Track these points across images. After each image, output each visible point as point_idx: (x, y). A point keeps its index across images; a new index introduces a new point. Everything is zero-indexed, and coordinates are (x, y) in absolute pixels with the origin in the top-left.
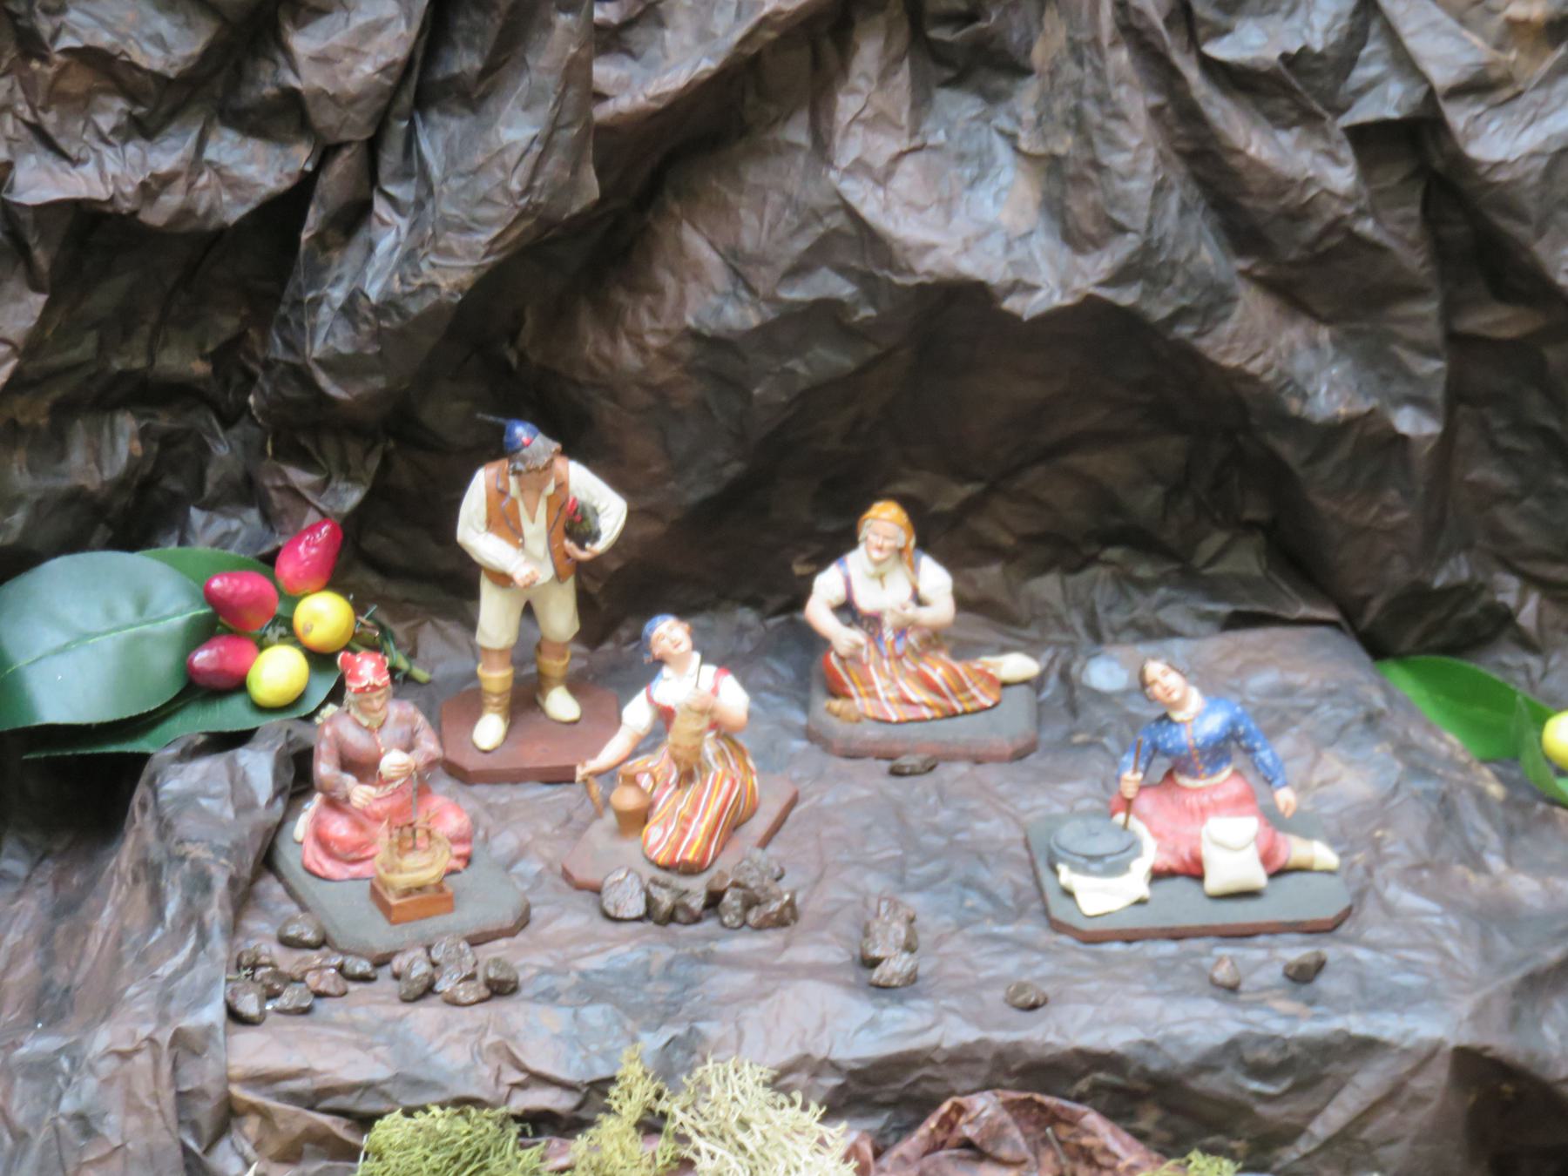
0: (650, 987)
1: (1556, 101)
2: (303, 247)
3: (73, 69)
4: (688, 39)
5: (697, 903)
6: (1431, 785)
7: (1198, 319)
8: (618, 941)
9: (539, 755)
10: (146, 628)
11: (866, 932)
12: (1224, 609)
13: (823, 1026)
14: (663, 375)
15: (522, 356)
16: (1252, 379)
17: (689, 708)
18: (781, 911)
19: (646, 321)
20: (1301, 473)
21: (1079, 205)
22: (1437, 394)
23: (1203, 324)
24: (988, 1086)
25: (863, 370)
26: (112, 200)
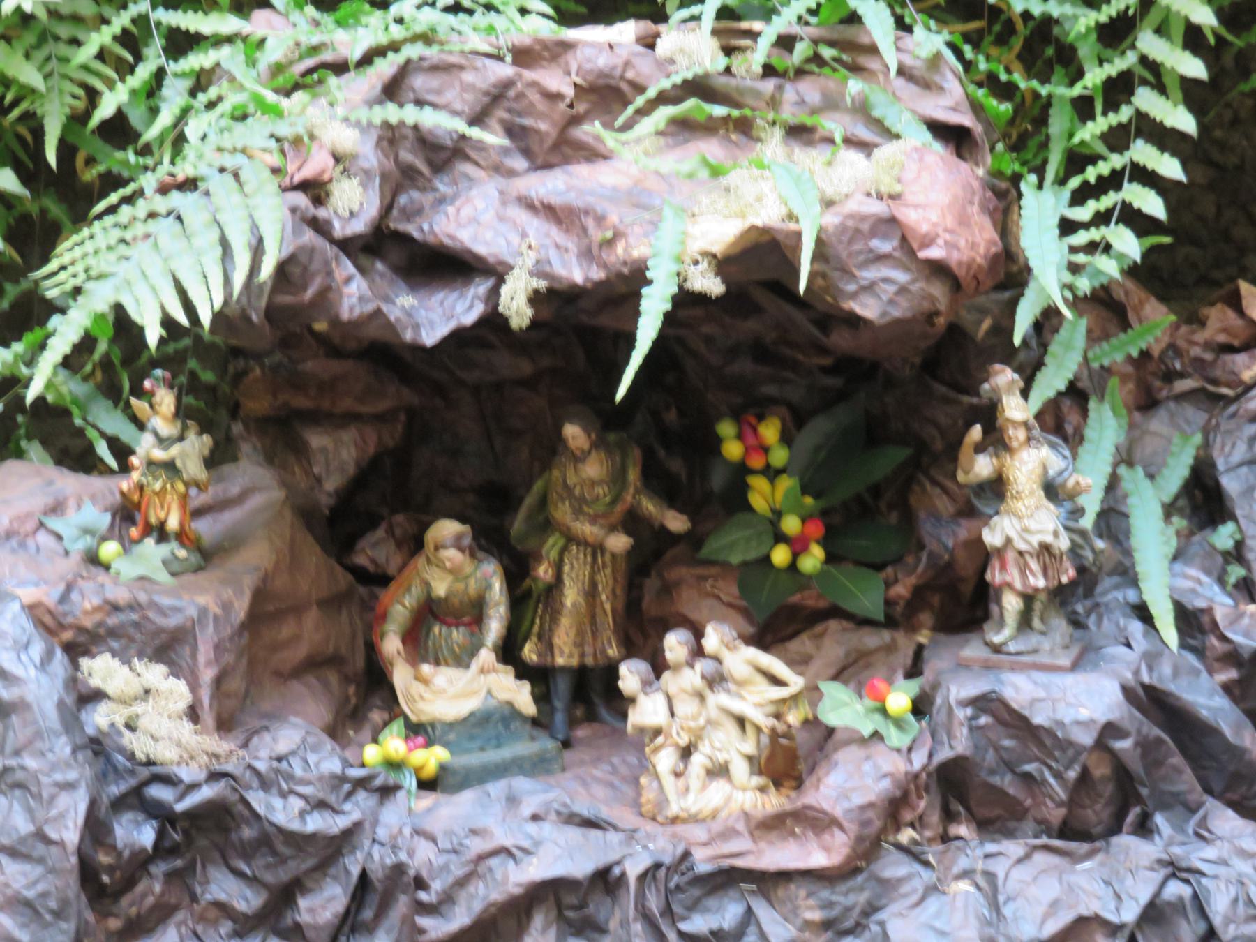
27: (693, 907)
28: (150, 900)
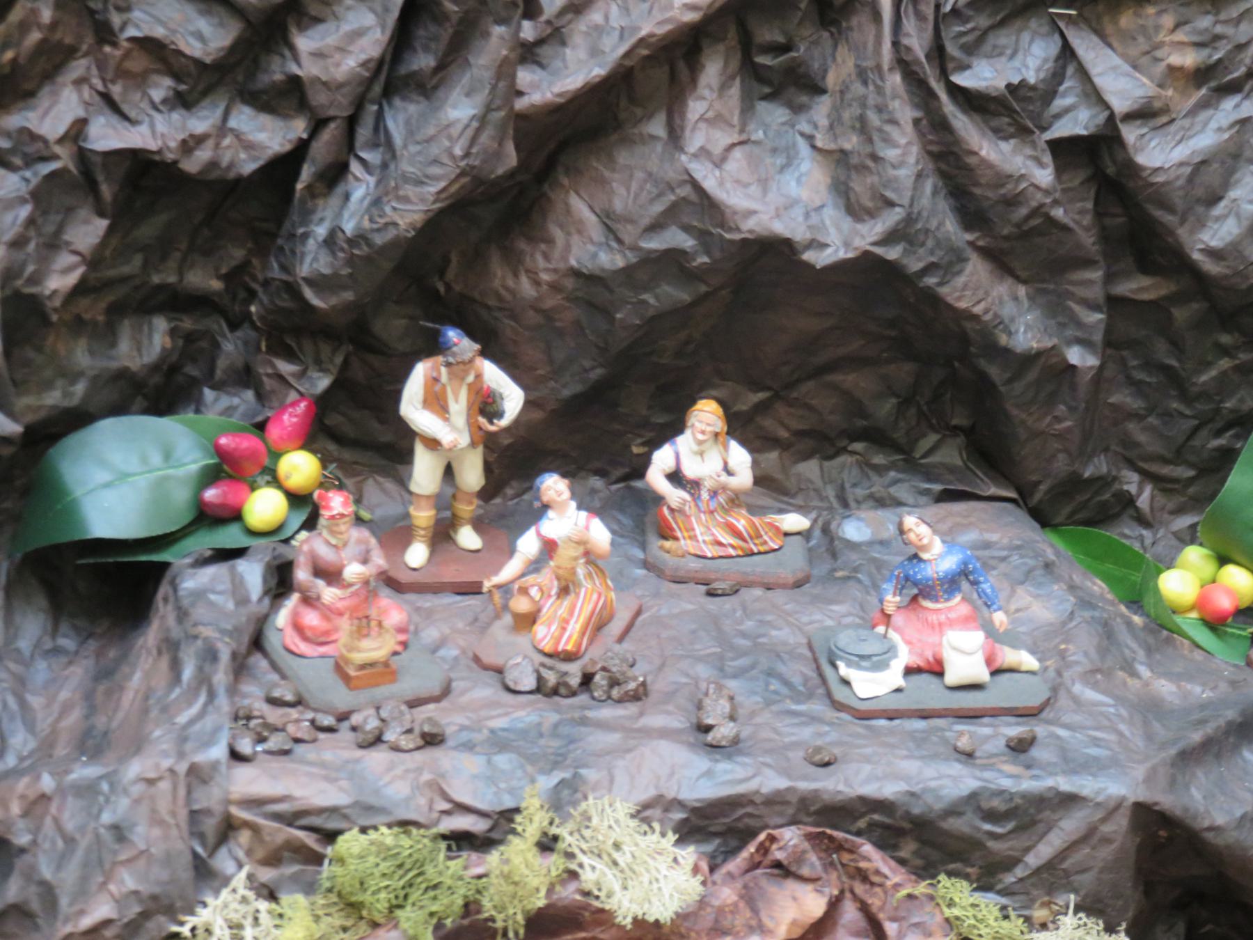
0: (542, 742)
1: (1198, 128)
2: (297, 195)
3: (135, 54)
4: (582, 54)
5: (575, 681)
6: (1097, 614)
7: (941, 272)
8: (522, 706)
9: (452, 573)
10: (171, 471)
11: (699, 706)
12: (937, 487)
13: (672, 774)
14: (550, 302)
15: (448, 287)
16: (975, 318)
17: (570, 539)
18: (636, 690)
19: (541, 262)
20: (1002, 389)
21: (860, 187)
22: (1098, 337)
23: (944, 275)
24: (793, 822)
25: (693, 304)
26: (159, 152)
27: (972, 49)
28: (35, 36)
